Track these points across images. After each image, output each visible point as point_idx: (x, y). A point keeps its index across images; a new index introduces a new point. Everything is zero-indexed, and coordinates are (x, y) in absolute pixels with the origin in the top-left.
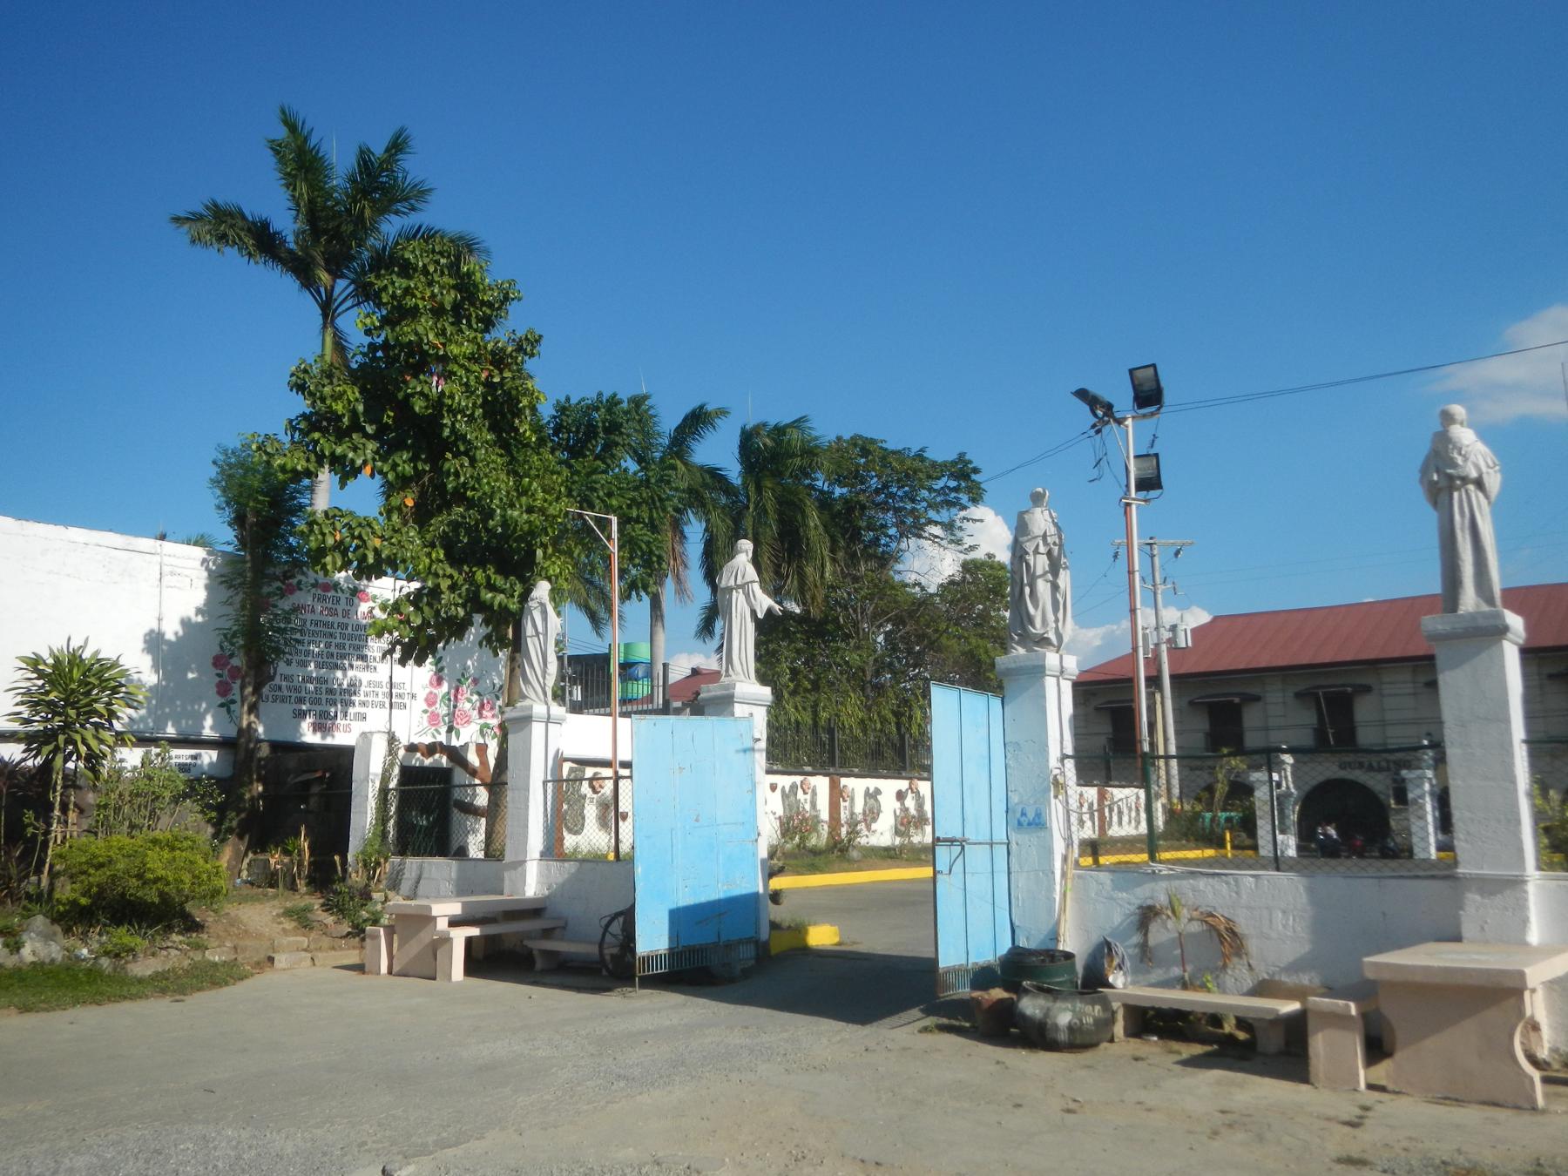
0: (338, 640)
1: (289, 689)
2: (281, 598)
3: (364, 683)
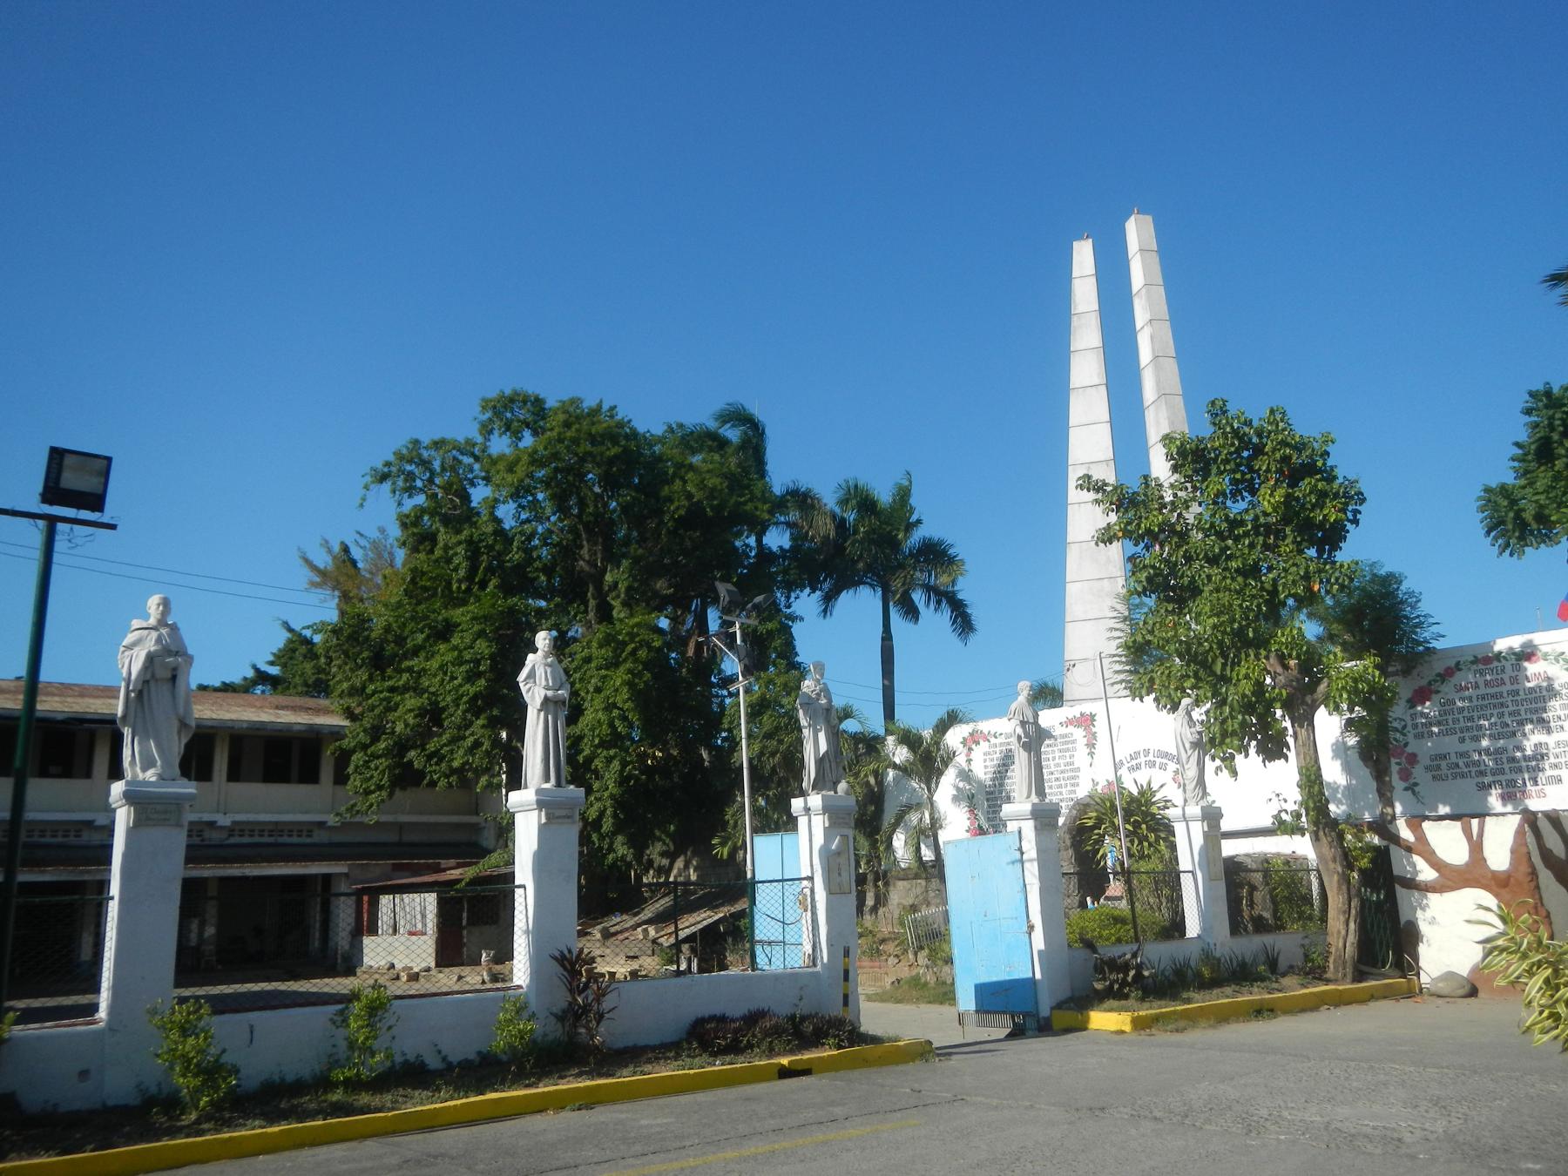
0: (1511, 708)
1: (1467, 765)
2: (1442, 683)
3: (1552, 745)
